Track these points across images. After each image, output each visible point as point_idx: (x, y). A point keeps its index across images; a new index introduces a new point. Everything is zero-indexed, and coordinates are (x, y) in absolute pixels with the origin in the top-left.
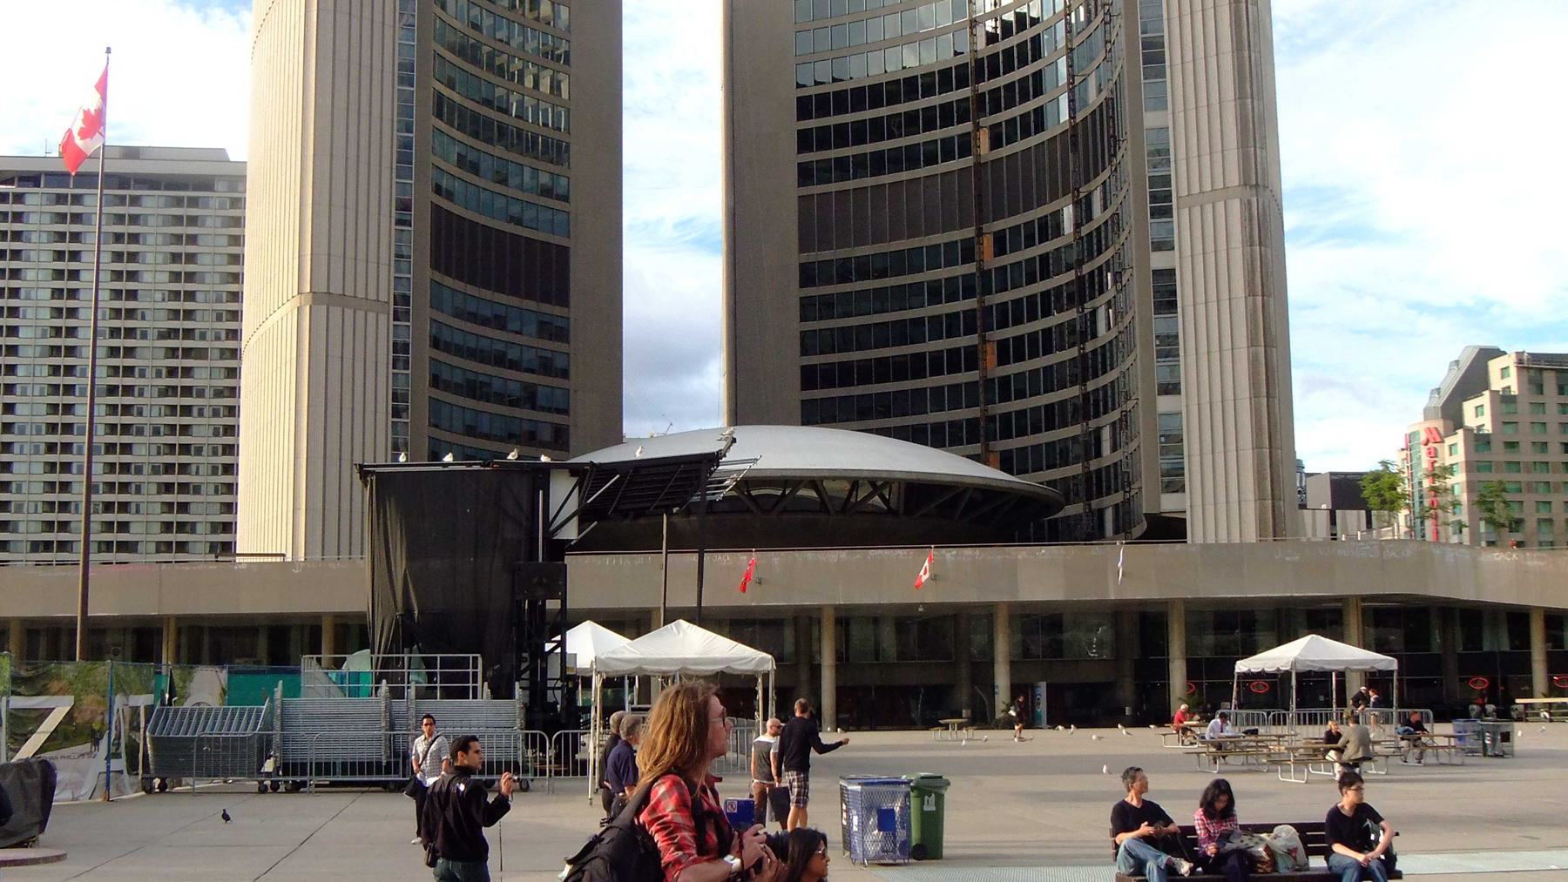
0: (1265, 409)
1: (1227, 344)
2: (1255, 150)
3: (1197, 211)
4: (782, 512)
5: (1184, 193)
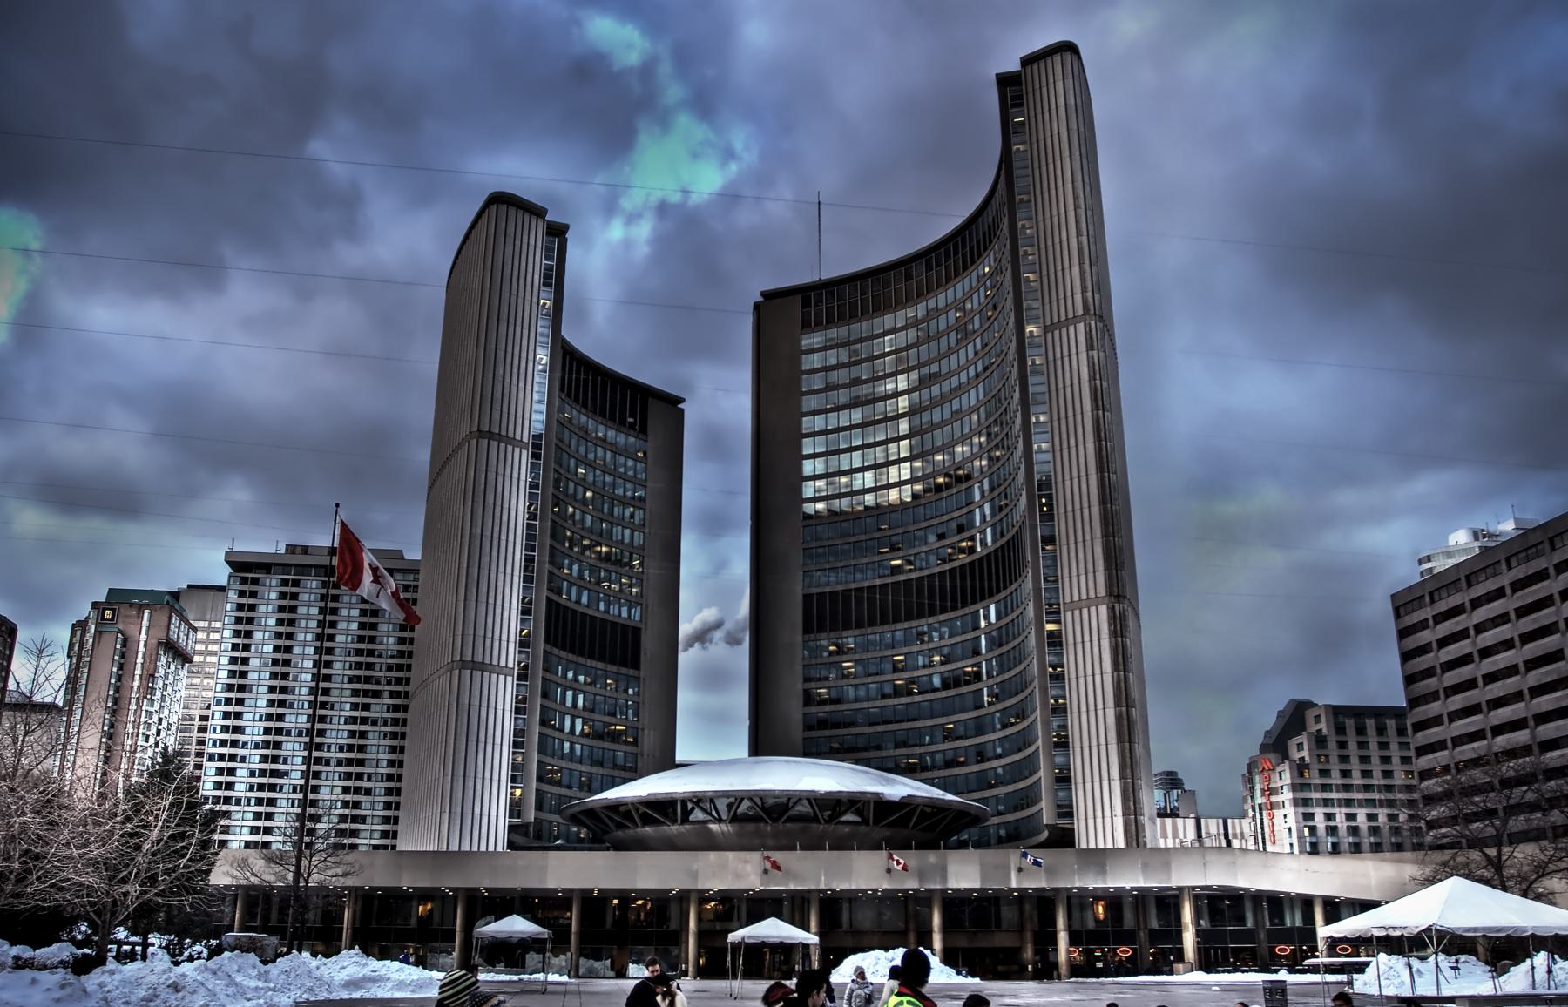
0: (1127, 751)
1: (1100, 706)
3: (1077, 612)
5: (1068, 600)
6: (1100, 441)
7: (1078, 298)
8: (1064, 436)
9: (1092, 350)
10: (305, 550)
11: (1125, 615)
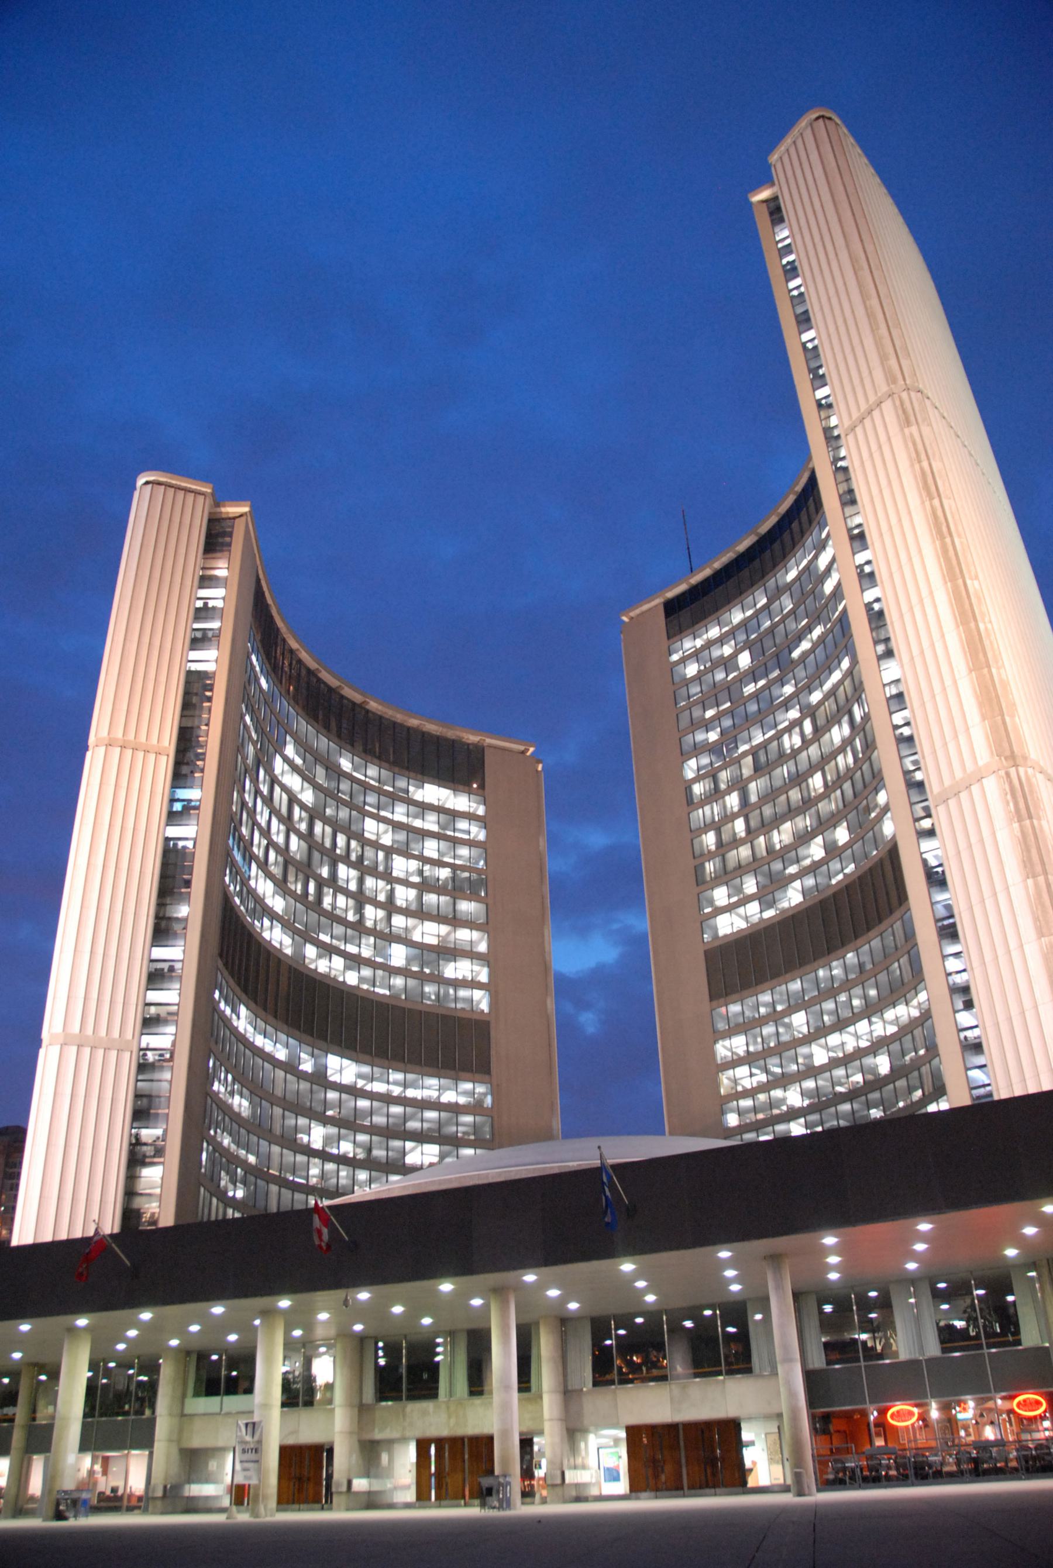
6: (942, 537)
9: (908, 423)
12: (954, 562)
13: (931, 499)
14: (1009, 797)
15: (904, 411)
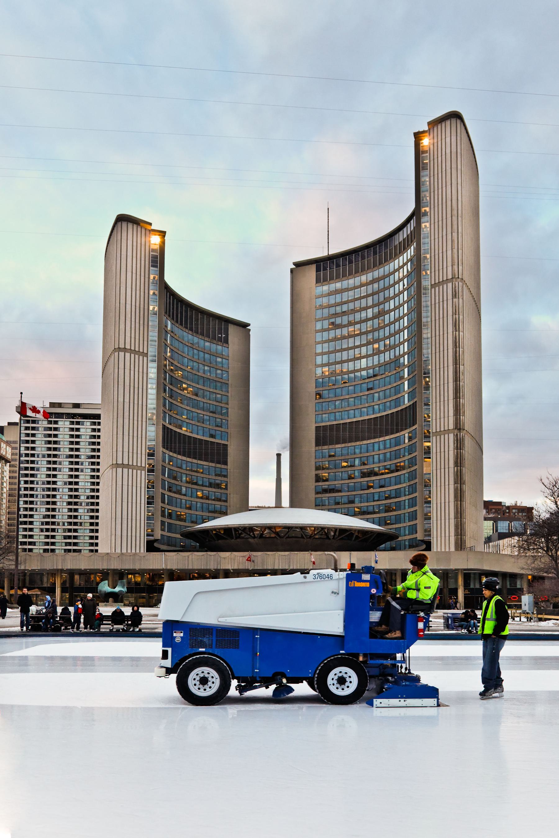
2: (460, 417)
4: (287, 538)
7: (450, 269)
8: (438, 346)
10: (60, 405)
11: (463, 439)
12: (458, 358)
13: (456, 331)
14: (456, 442)
15: (455, 292)
